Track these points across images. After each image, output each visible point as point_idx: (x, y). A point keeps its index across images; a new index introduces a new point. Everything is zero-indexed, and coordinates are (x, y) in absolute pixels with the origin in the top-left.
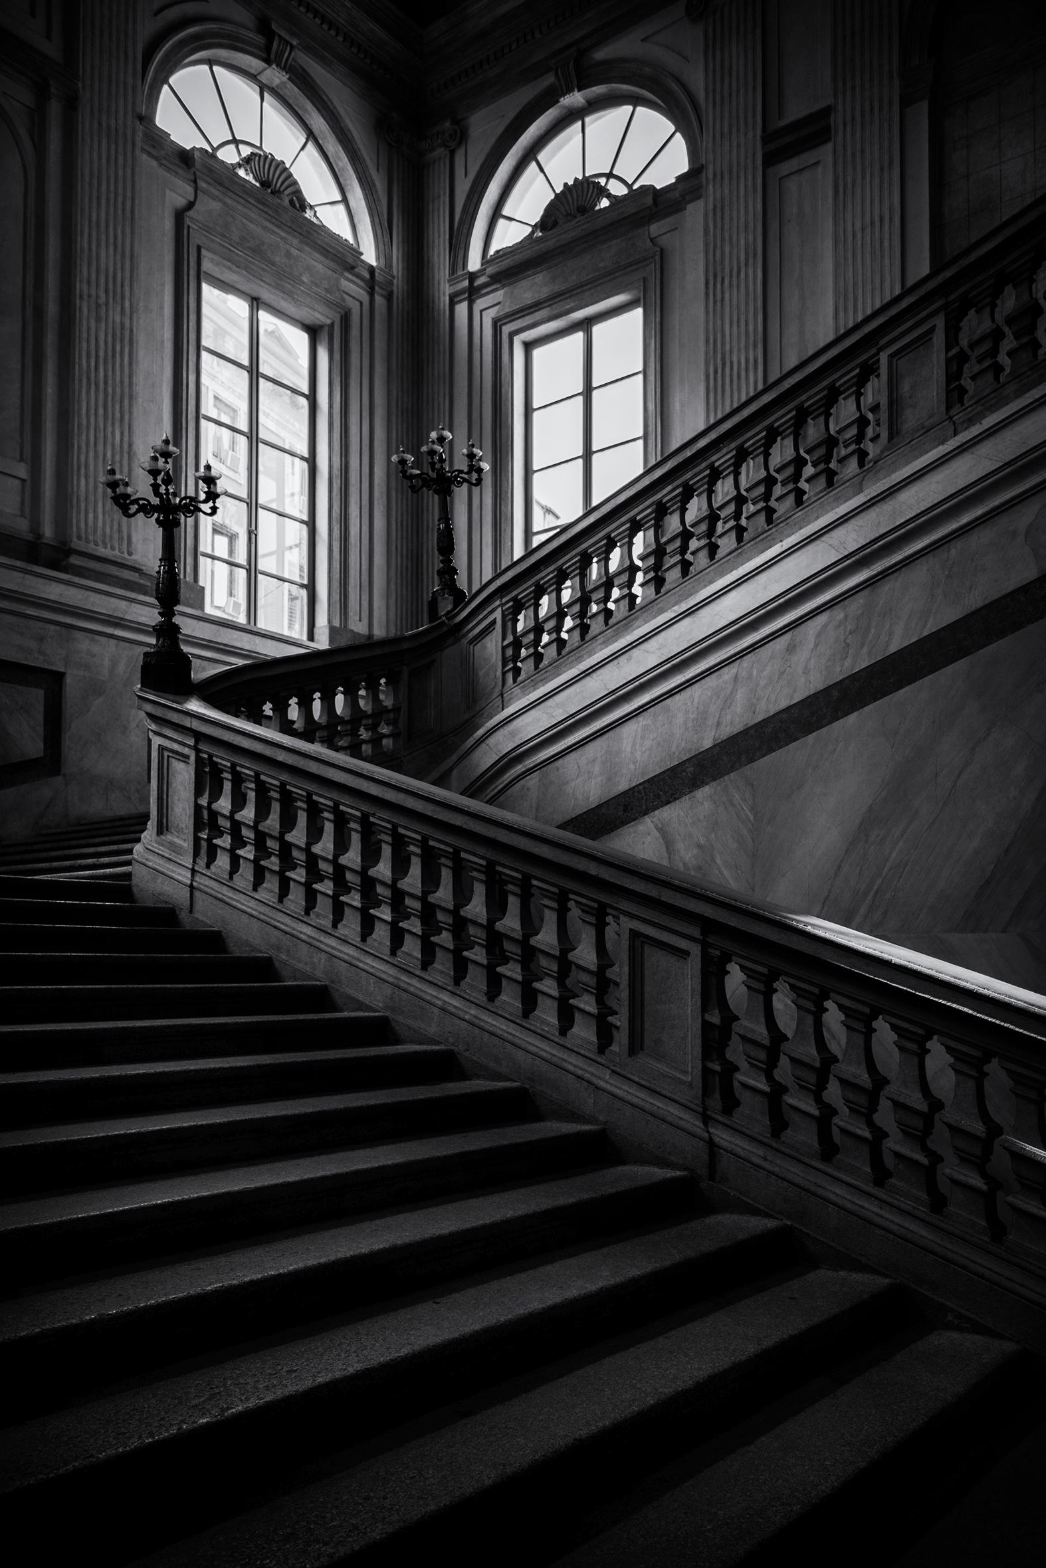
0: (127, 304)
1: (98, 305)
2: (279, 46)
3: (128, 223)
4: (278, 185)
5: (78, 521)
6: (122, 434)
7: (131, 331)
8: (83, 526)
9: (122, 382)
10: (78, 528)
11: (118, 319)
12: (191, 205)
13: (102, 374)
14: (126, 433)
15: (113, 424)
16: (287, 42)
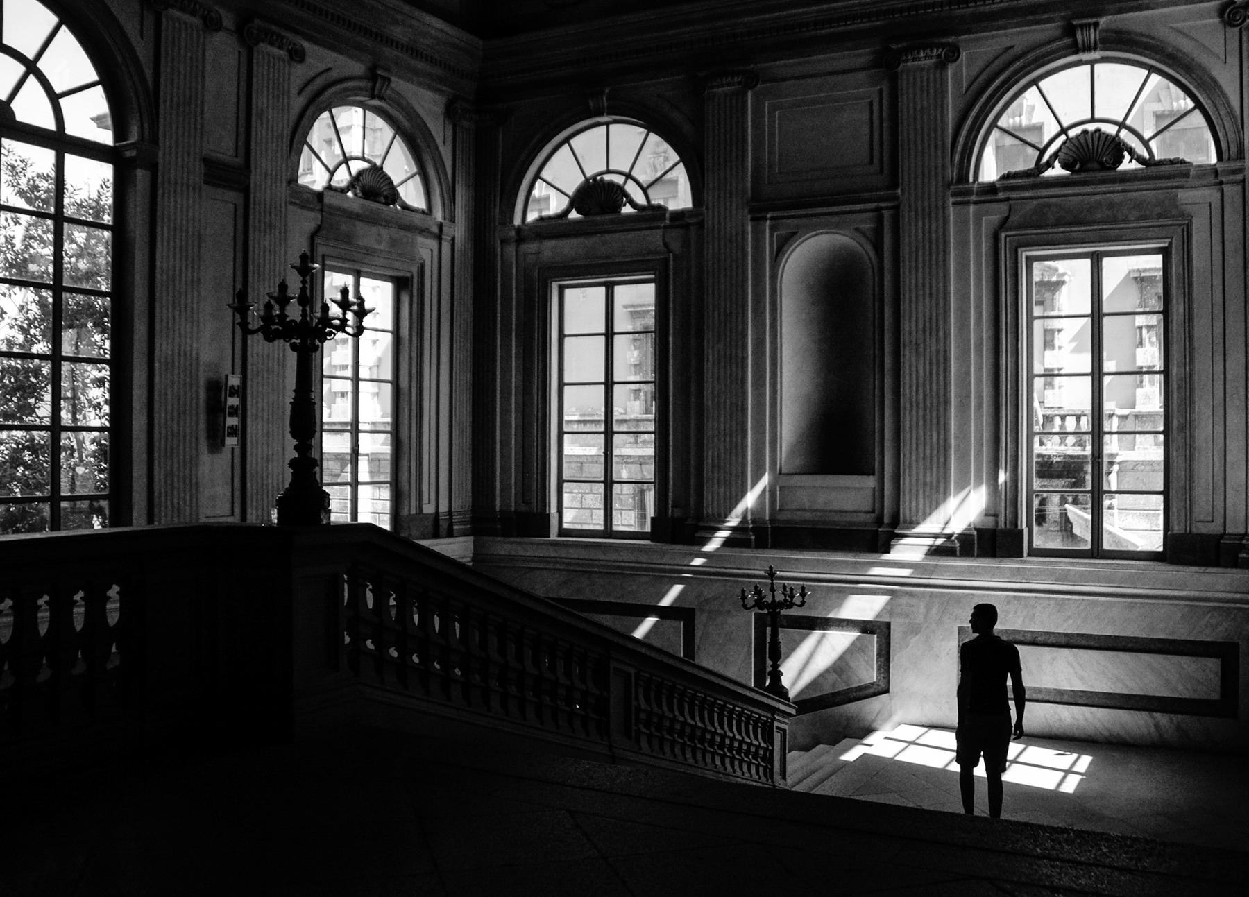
0: (941, 333)
1: (917, 345)
2: (1082, 34)
3: (941, 271)
4: (1100, 150)
5: (904, 509)
6: (938, 435)
7: (945, 351)
8: (907, 512)
9: (938, 393)
10: (904, 515)
11: (933, 348)
12: (1007, 218)
13: (921, 396)
14: (942, 432)
15: (931, 429)
16: (1089, 25)
